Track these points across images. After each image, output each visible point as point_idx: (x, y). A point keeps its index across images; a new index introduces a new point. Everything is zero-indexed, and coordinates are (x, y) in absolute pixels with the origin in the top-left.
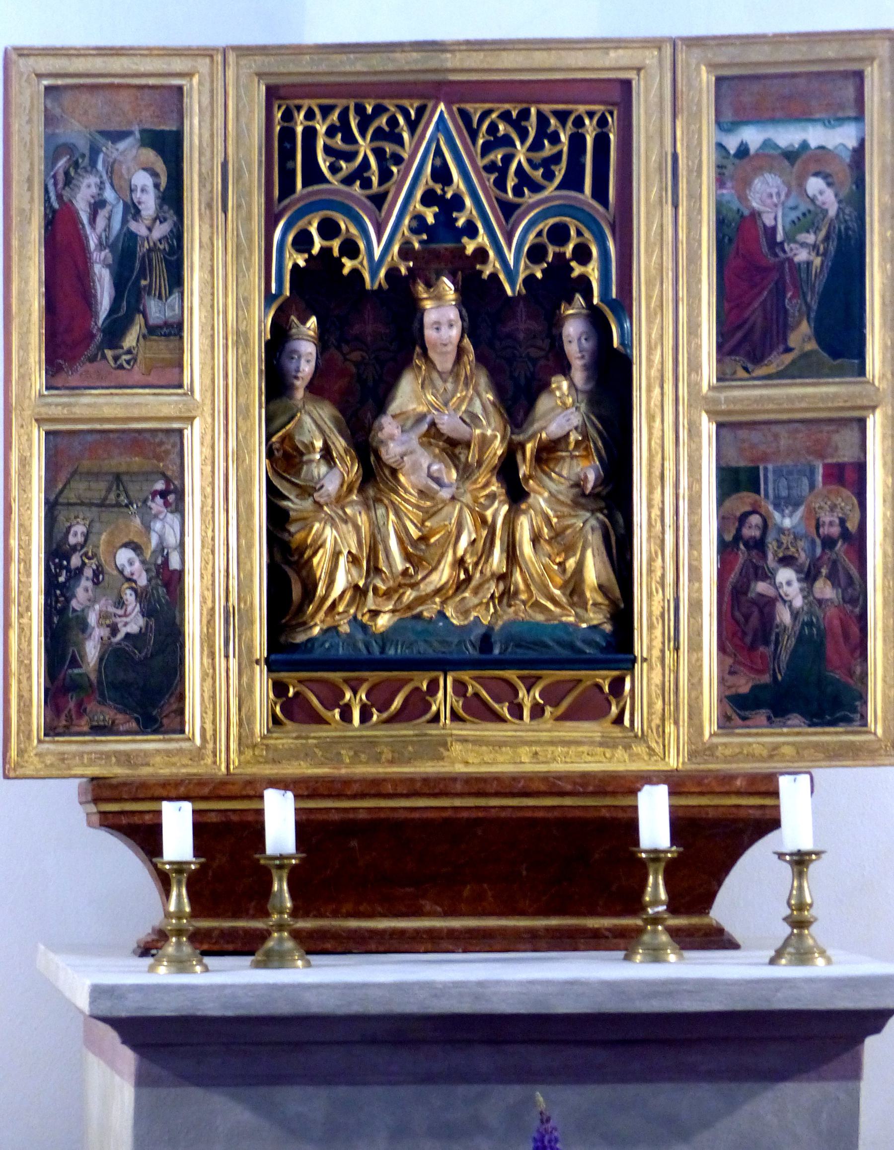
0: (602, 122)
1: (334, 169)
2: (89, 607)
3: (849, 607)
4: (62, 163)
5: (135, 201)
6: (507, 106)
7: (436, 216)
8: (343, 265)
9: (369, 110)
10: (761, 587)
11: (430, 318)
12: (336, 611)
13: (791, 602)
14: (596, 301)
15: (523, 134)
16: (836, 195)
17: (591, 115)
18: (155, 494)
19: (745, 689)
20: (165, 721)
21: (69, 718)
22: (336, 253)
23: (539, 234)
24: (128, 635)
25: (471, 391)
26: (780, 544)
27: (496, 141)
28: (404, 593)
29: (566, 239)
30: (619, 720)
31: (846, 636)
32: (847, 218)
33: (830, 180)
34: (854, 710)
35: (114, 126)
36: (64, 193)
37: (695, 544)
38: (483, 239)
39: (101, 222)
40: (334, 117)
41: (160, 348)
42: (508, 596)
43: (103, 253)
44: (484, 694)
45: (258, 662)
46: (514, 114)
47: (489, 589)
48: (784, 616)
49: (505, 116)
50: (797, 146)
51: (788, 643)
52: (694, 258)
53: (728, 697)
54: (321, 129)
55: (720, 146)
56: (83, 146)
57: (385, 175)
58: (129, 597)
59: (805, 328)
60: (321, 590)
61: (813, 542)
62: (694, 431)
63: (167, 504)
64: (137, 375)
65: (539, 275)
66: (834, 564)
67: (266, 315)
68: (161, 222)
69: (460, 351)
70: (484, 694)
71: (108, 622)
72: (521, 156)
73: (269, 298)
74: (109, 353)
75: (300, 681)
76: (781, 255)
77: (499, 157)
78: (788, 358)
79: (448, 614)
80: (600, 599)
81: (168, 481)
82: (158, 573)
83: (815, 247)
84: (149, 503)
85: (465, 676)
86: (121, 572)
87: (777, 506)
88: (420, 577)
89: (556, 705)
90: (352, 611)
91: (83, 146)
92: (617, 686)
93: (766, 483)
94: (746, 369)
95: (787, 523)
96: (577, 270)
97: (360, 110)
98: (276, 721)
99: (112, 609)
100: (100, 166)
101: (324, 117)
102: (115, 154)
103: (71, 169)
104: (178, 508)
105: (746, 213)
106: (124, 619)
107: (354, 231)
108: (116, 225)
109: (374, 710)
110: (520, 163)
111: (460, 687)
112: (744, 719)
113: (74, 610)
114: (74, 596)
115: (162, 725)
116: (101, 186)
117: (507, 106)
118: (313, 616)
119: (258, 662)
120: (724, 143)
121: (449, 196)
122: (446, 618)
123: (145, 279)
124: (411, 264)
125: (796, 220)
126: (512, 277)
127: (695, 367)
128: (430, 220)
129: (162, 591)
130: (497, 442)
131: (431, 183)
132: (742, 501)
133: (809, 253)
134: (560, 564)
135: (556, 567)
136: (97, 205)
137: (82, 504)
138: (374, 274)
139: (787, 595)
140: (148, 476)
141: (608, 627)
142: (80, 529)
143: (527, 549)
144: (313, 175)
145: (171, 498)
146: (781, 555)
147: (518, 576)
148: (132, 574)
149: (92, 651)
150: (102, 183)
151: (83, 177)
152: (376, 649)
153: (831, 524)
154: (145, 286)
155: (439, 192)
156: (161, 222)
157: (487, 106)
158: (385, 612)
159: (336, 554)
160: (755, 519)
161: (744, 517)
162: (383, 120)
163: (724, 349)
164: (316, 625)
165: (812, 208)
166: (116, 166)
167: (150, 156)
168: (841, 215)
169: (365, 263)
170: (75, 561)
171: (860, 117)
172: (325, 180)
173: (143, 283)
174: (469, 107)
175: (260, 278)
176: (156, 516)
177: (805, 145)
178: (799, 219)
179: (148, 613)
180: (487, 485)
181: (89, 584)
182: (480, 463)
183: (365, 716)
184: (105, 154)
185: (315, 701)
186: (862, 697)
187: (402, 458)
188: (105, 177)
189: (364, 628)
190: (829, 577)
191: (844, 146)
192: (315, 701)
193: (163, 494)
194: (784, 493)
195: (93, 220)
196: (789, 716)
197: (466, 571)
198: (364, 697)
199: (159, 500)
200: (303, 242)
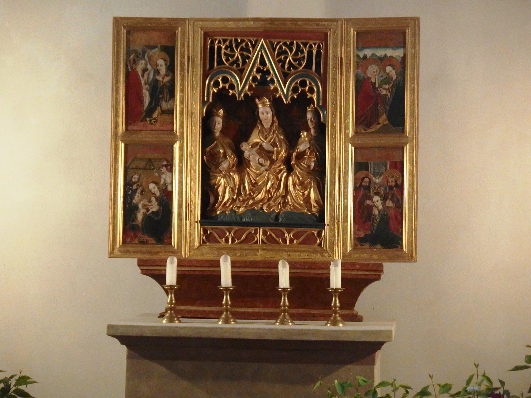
0: (319, 47)
1: (227, 60)
2: (139, 202)
3: (397, 209)
4: (132, 57)
5: (158, 69)
7: (261, 76)
8: (229, 92)
9: (239, 41)
10: (368, 202)
11: (260, 110)
12: (226, 206)
13: (378, 207)
14: (315, 106)
15: (291, 51)
16: (396, 72)
17: (315, 44)
18: (163, 166)
19: (362, 236)
20: (165, 241)
21: (132, 239)
22: (227, 88)
23: (296, 83)
24: (153, 212)
25: (275, 135)
26: (374, 187)
27: (282, 52)
28: (249, 201)
30: (320, 245)
31: (396, 218)
32: (399, 80)
33: (394, 67)
34: (398, 243)
35: (152, 43)
36: (133, 66)
37: (346, 187)
38: (276, 84)
39: (146, 76)
40: (228, 42)
41: (166, 117)
42: (285, 203)
43: (146, 86)
44: (273, 235)
45: (197, 222)
46: (288, 43)
47: (279, 200)
48: (376, 212)
49: (285, 44)
50: (383, 56)
51: (377, 221)
52: (347, 92)
53: (357, 238)
54: (223, 47)
55: (358, 56)
56: (140, 50)
57: (244, 63)
58: (153, 199)
59: (384, 116)
60: (220, 199)
61: (386, 188)
62: (346, 150)
63: (167, 169)
64: (158, 126)
65: (295, 97)
66: (393, 195)
68: (167, 76)
70: (273, 235)
71: (145, 207)
72: (290, 58)
73: (204, 103)
74: (148, 119)
75: (212, 229)
76: (377, 92)
77: (283, 57)
78: (379, 126)
79: (264, 208)
80: (315, 205)
81: (168, 161)
82: (164, 192)
83: (388, 89)
84: (161, 169)
85: (267, 229)
86: (151, 191)
87: (374, 176)
88: (254, 196)
90: (231, 206)
91: (140, 50)
92: (320, 234)
93: (371, 168)
94: (364, 130)
95: (377, 181)
96: (309, 95)
97: (236, 40)
98: (204, 242)
99: (147, 203)
100: (146, 57)
101: (224, 43)
102: (151, 53)
103: (136, 58)
104: (171, 171)
105: (366, 78)
106: (152, 207)
109: (236, 239)
110: (290, 60)
111: (265, 233)
112: (361, 245)
113: (134, 203)
114: (134, 198)
115: (164, 242)
116: (146, 64)
117: (285, 41)
118: (218, 207)
119: (197, 222)
120: (359, 54)
121: (265, 70)
122: (263, 209)
123: (161, 95)
124: (252, 92)
125: (382, 80)
126: (286, 98)
127: (347, 128)
128: (259, 77)
129: (165, 197)
130: (283, 152)
131: (259, 66)
132: (362, 174)
133: (386, 91)
134: (302, 193)
135: (301, 194)
136: (145, 70)
137: (137, 168)
138: (240, 95)
139: (377, 205)
140: (160, 160)
141: (317, 214)
142: (136, 177)
143: (291, 188)
144: (220, 62)
145: (169, 167)
146: (375, 192)
147: (289, 197)
148: (154, 192)
149: (140, 216)
150: (146, 62)
151: (140, 61)
152: (239, 220)
153: (392, 182)
154: (161, 97)
155: (262, 68)
156: (167, 76)
157: (278, 40)
158: (242, 207)
159: (225, 188)
160: (367, 180)
161: (364, 178)
163: (358, 123)
164: (218, 210)
165: (388, 77)
166: (152, 58)
167: (164, 54)
168: (397, 79)
169: (237, 91)
170: (135, 187)
171: (404, 47)
172: (224, 64)
173: (160, 96)
174: (273, 41)
175: (200, 96)
176: (163, 173)
178: (383, 80)
179: (160, 204)
180: (280, 166)
181: (139, 195)
182: (277, 159)
183: (233, 241)
184: (148, 53)
185: (216, 236)
186: (401, 240)
187: (249, 156)
188: (147, 61)
189: (235, 212)
190: (391, 199)
191: (399, 56)
192: (216, 236)
193: (166, 166)
194: (376, 171)
195: (143, 76)
196: (377, 245)
197: (271, 195)
198: (233, 235)
199: (164, 168)
200: (216, 84)
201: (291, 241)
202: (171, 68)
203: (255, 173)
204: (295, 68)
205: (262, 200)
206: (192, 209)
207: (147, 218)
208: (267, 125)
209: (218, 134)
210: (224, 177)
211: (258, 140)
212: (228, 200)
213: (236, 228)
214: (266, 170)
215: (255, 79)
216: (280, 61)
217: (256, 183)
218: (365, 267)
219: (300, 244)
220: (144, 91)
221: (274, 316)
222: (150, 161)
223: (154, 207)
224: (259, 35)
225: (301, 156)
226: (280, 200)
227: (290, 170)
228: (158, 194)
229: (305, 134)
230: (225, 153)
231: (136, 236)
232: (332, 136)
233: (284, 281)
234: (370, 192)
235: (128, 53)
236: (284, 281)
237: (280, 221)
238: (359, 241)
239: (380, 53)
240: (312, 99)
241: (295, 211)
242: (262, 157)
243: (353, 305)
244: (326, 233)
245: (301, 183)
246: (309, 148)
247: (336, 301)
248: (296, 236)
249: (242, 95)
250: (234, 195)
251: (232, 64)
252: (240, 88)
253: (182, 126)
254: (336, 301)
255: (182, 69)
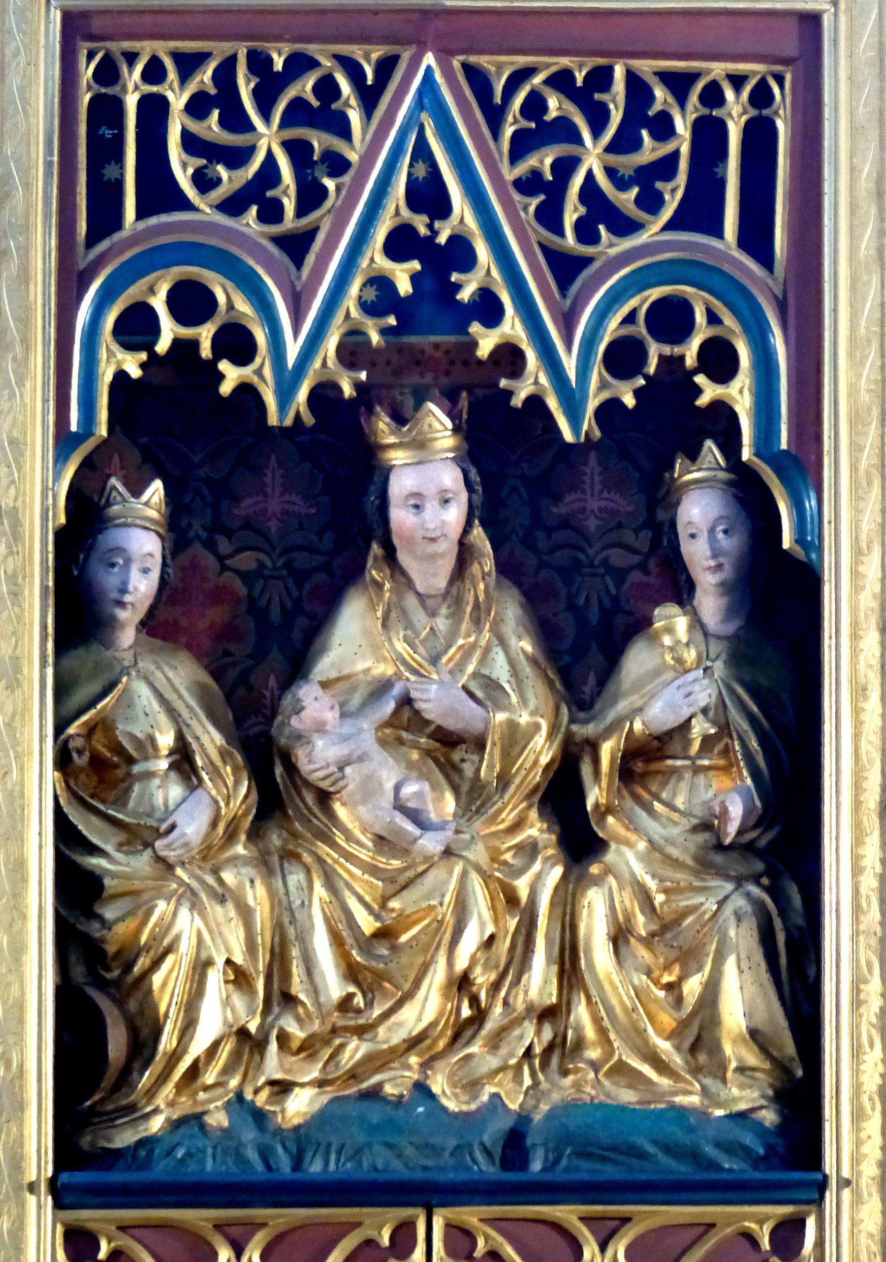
6: (565, 61)
7: (415, 279)
8: (221, 377)
9: (279, 64)
12: (199, 1082)
14: (746, 454)
22: (206, 352)
40: (205, 76)
45: (32, 1188)
46: (580, 78)
47: (521, 1037)
54: (178, 100)
60: (167, 1041)
65: (629, 401)
67: (57, 476)
79: (436, 1089)
80: (752, 1059)
88: (377, 1012)
90: (234, 1083)
101: (184, 78)
107: (243, 306)
117: (565, 61)
118: (151, 1093)
119: (32, 1188)
121: (442, 239)
122: (431, 1096)
128: (404, 287)
131: (405, 213)
134: (670, 987)
138: (285, 395)
147: (581, 1013)
155: (423, 231)
175: (45, 401)
182: (504, 781)
187: (341, 769)
189: (259, 1117)
197: (474, 1001)
252: (293, 350)
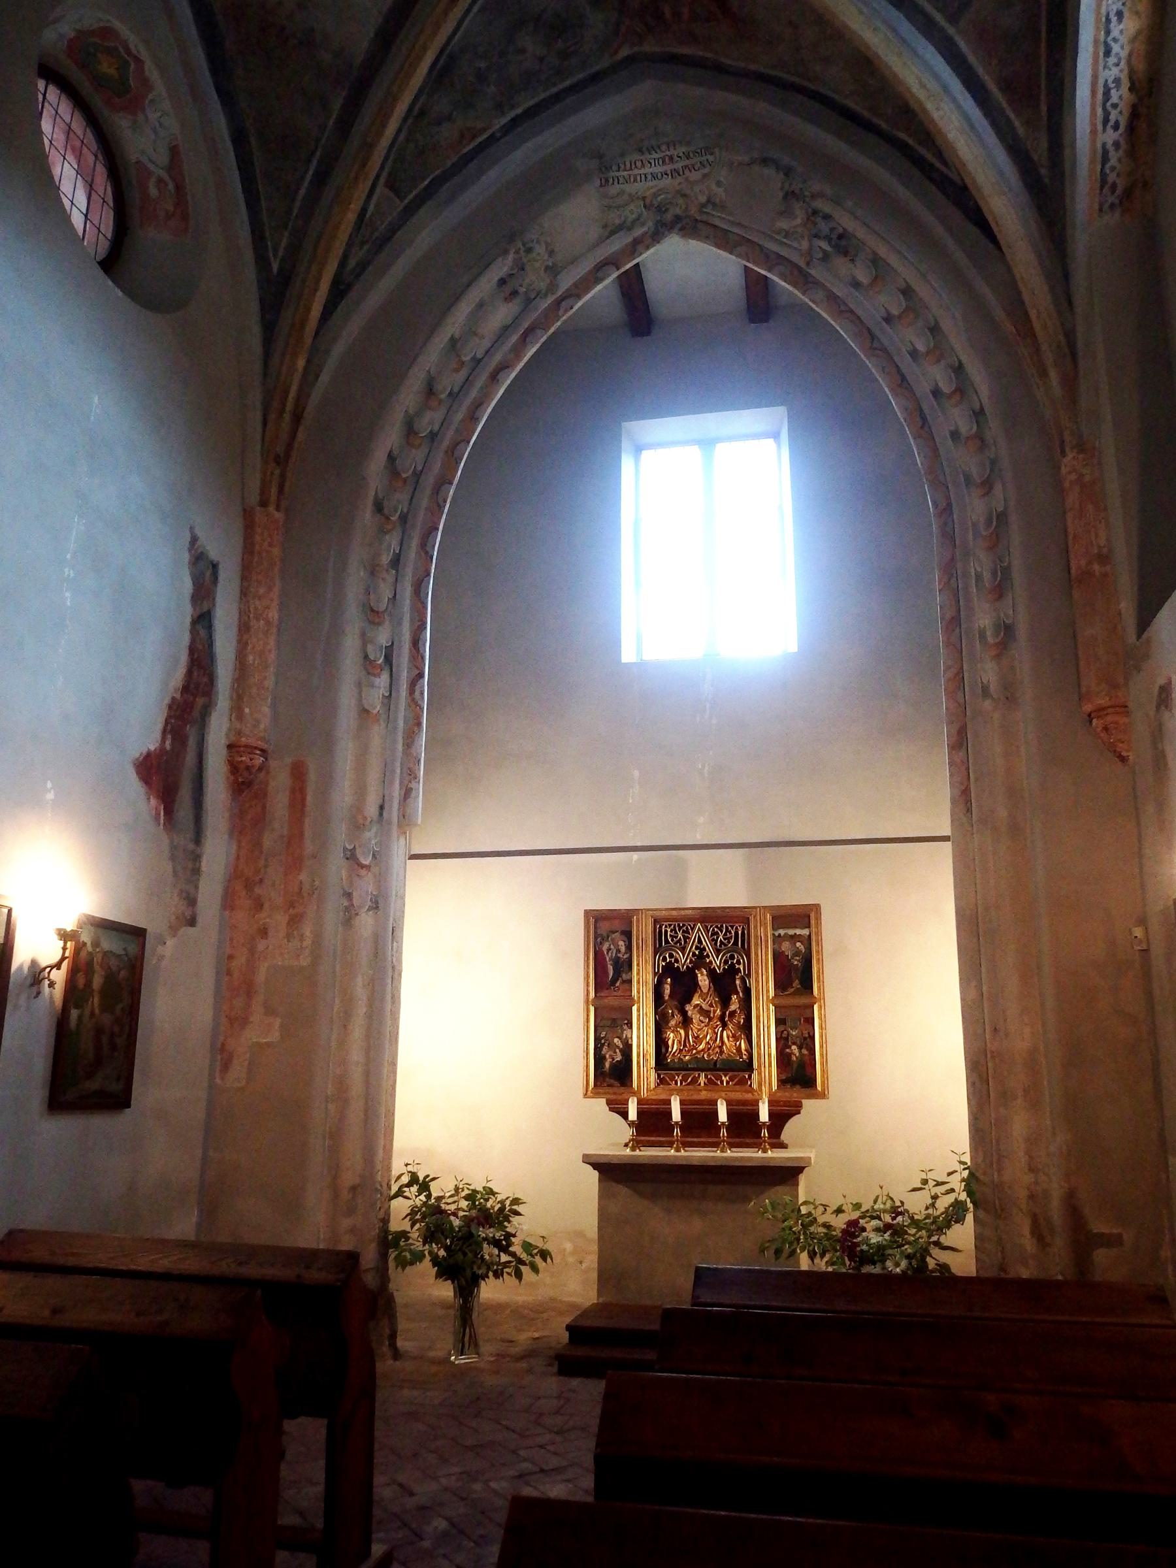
0: (743, 928)
1: (672, 940)
4: (599, 939)
6: (717, 924)
10: (788, 1050)
11: (699, 979)
15: (722, 932)
17: (740, 926)
18: (625, 1024)
21: (601, 1083)
23: (727, 957)
24: (617, 1061)
25: (712, 998)
27: (714, 933)
29: (734, 959)
30: (751, 1085)
34: (813, 1084)
35: (614, 928)
37: (769, 1039)
38: (711, 958)
39: (610, 954)
40: (672, 927)
41: (626, 986)
42: (722, 1052)
44: (713, 1078)
48: (794, 1058)
49: (717, 927)
51: (795, 1066)
54: (669, 930)
55: (774, 934)
56: (605, 935)
57: (685, 942)
58: (618, 1051)
60: (670, 1050)
62: (768, 1009)
63: (628, 1026)
64: (620, 993)
66: (807, 1044)
67: (655, 978)
69: (710, 988)
70: (713, 1078)
72: (721, 937)
73: (655, 974)
74: (612, 988)
78: (793, 990)
85: (708, 1073)
89: (732, 1081)
91: (605, 935)
95: (794, 1033)
96: (737, 966)
97: (679, 925)
98: (658, 1085)
99: (613, 1054)
104: (631, 1028)
107: (677, 956)
108: (614, 955)
111: (706, 1076)
117: (717, 924)
127: (768, 991)
128: (697, 953)
130: (718, 1011)
132: (782, 1028)
136: (609, 950)
138: (683, 967)
141: (747, 1061)
144: (667, 942)
147: (724, 1047)
149: (607, 1065)
160: (785, 1032)
161: (783, 1031)
162: (685, 928)
170: (603, 1041)
171: (809, 927)
176: (625, 1030)
177: (795, 934)
180: (716, 1023)
183: (681, 1084)
185: (668, 1079)
189: (682, 1059)
190: (805, 1048)
192: (668, 1079)
193: (627, 1024)
195: (608, 953)
199: (626, 1026)
200: (664, 959)
201: (728, 1083)
202: (629, 948)
203: (697, 1028)
204: (725, 945)
205: (703, 1050)
206: (648, 1058)
207: (613, 1066)
208: (705, 991)
209: (667, 998)
210: (673, 1032)
211: (699, 1002)
212: (676, 1050)
213: (683, 1073)
214: (706, 1026)
215: (694, 954)
216: (713, 940)
217: (698, 1036)
218: (787, 1103)
219: (734, 1085)
220: (609, 966)
221: (715, 1145)
222: (614, 1020)
223: (619, 1058)
224: (695, 920)
225: (732, 1014)
226: (717, 1049)
227: (724, 1026)
228: (621, 1047)
229: (735, 996)
230: (673, 1013)
231: (604, 1081)
232: (756, 998)
233: (723, 1116)
234: (788, 1042)
235: (596, 938)
236: (723, 1116)
237: (718, 1066)
238: (782, 1082)
239: (791, 932)
240: (739, 969)
241: (730, 1058)
242: (701, 1015)
243: (778, 1135)
244: (755, 1076)
245: (734, 1036)
246: (739, 1008)
247: (765, 1133)
248: (731, 1079)
249: (685, 967)
250: (681, 1046)
251: (676, 943)
253: (638, 992)
254: (765, 1133)
255: (638, 948)
